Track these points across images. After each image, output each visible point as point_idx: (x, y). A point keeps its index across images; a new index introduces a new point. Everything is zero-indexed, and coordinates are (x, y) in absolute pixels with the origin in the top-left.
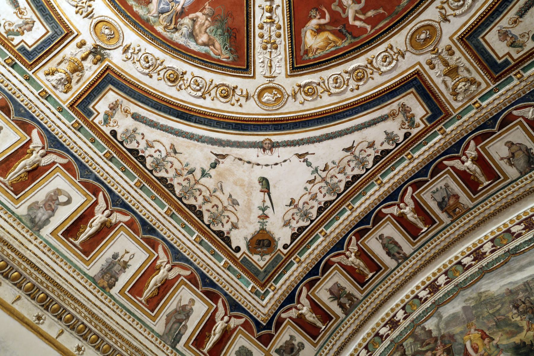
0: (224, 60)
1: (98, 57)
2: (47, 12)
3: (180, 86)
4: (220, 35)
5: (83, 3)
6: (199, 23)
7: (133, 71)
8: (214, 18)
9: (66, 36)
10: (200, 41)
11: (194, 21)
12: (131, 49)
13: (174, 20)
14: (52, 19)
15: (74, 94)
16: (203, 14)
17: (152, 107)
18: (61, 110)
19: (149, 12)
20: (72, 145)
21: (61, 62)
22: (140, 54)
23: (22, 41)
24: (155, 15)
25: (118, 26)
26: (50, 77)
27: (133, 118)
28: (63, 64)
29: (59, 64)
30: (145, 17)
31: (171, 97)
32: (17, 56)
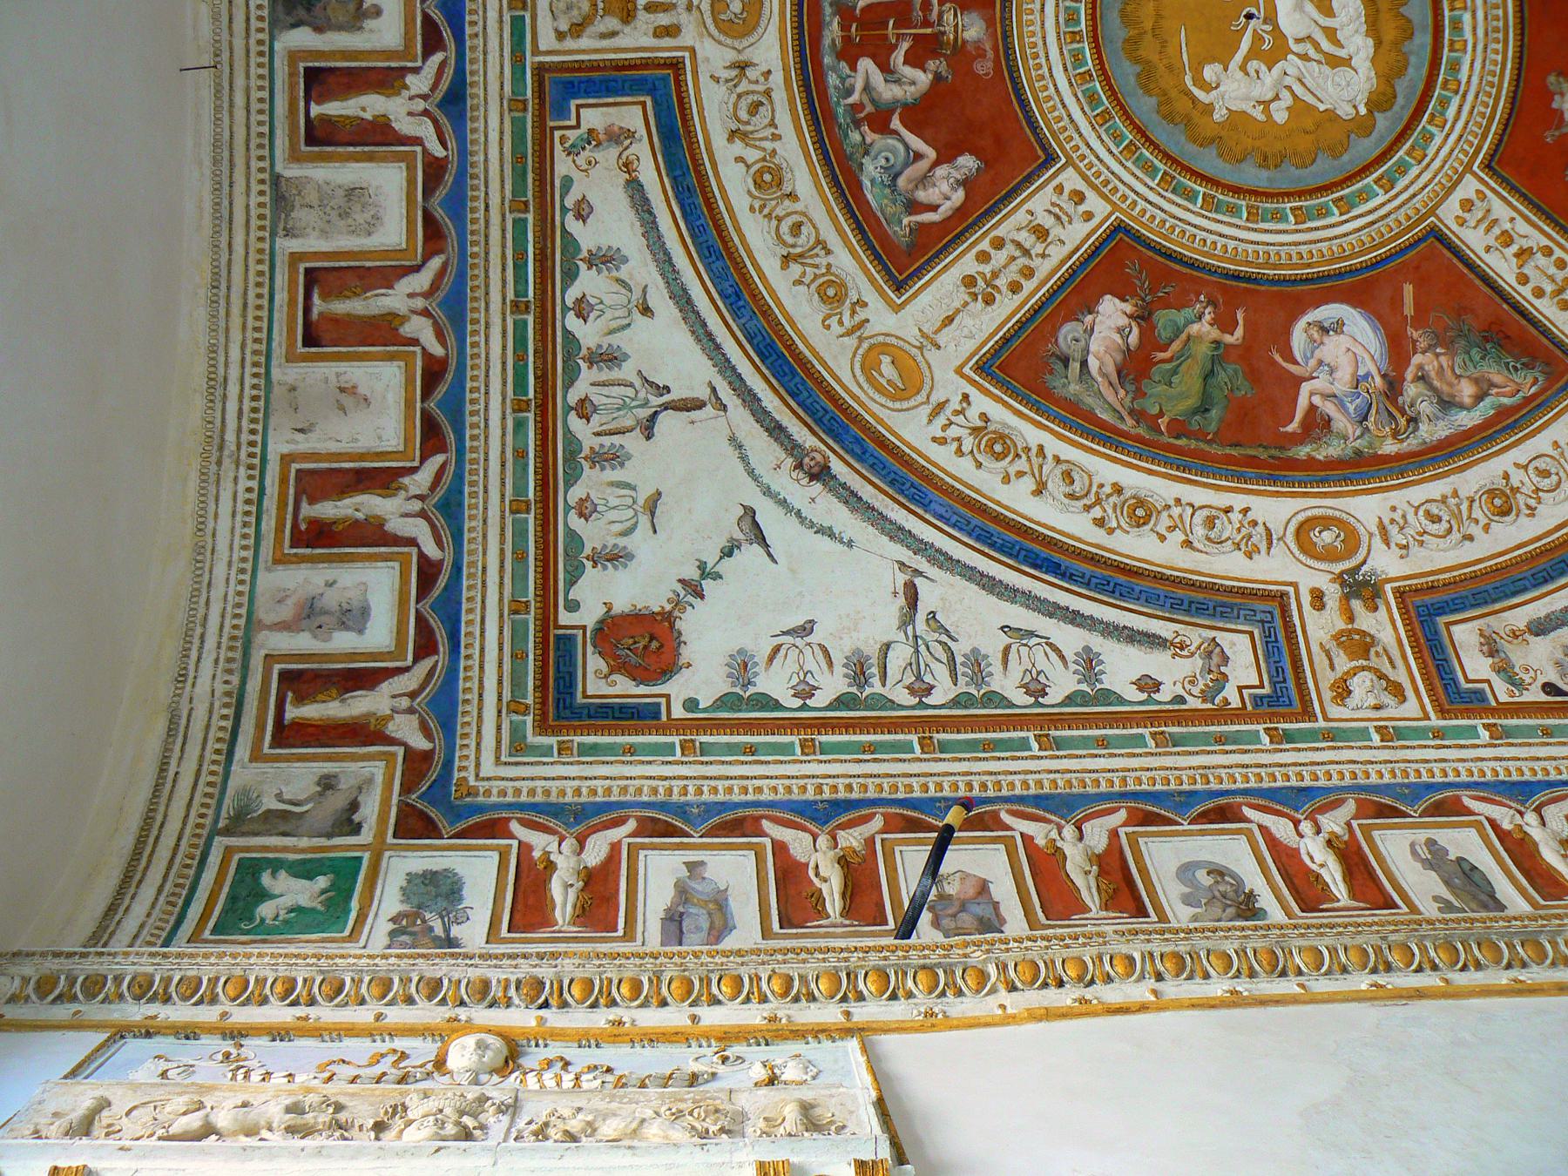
0: (1533, 390)
1: (1367, 593)
2: (1211, 605)
3: (1529, 507)
4: (1483, 358)
5: (1239, 530)
6: (1433, 374)
7: (1441, 557)
8: (1442, 340)
9: (1285, 610)
10: (1467, 401)
11: (1422, 378)
12: (1390, 527)
13: (1392, 409)
14: (1231, 606)
15: (1416, 690)
16: (1424, 352)
17: (1535, 586)
18: (1438, 734)
19: (1346, 438)
20: (1537, 766)
21: (1330, 659)
22: (1411, 517)
23: (1240, 688)
24: (1358, 433)
25: (1330, 512)
26: (1353, 701)
27: (1537, 635)
28: (1336, 661)
29: (1332, 667)
30: (1349, 452)
31: (1539, 539)
32: (1272, 717)
